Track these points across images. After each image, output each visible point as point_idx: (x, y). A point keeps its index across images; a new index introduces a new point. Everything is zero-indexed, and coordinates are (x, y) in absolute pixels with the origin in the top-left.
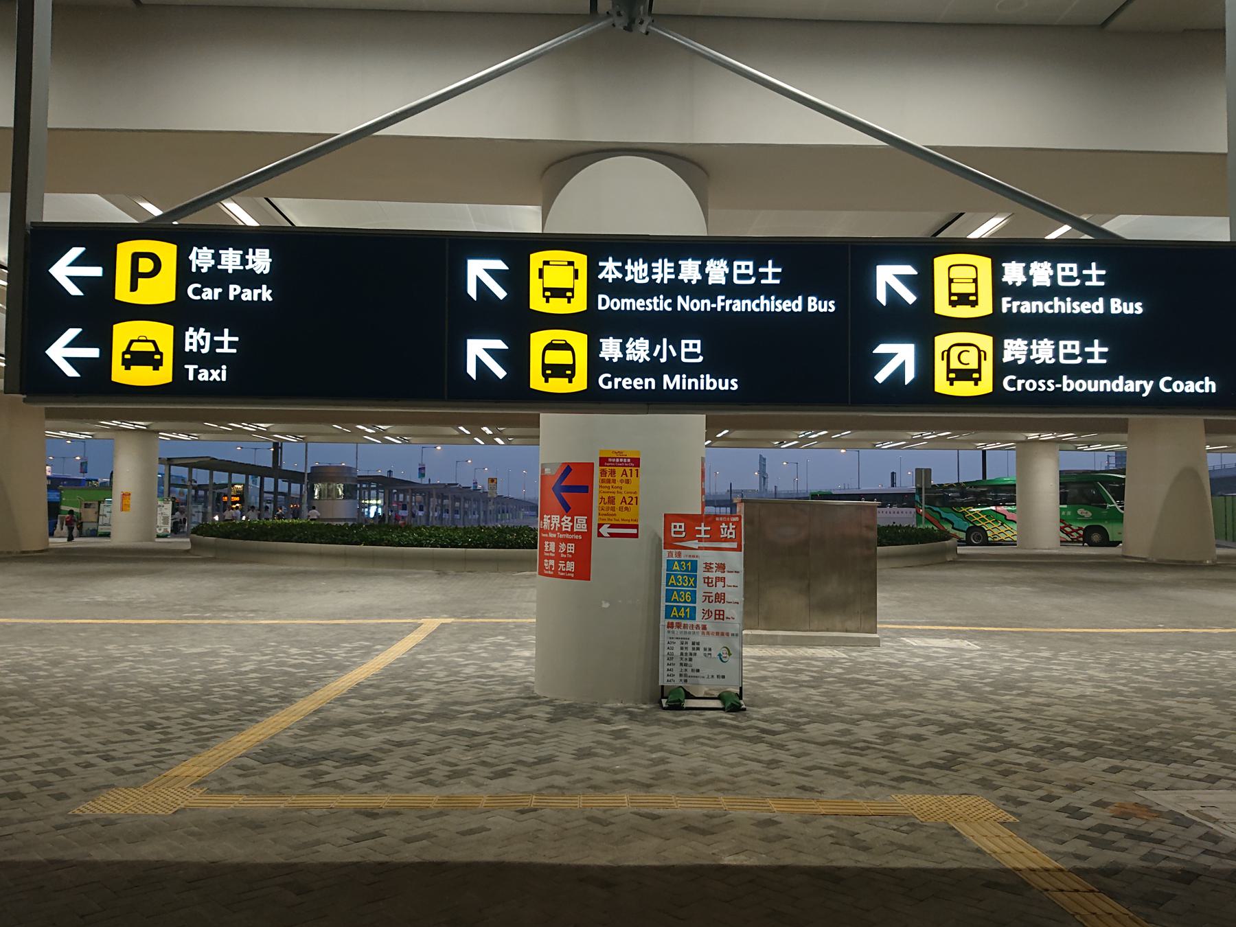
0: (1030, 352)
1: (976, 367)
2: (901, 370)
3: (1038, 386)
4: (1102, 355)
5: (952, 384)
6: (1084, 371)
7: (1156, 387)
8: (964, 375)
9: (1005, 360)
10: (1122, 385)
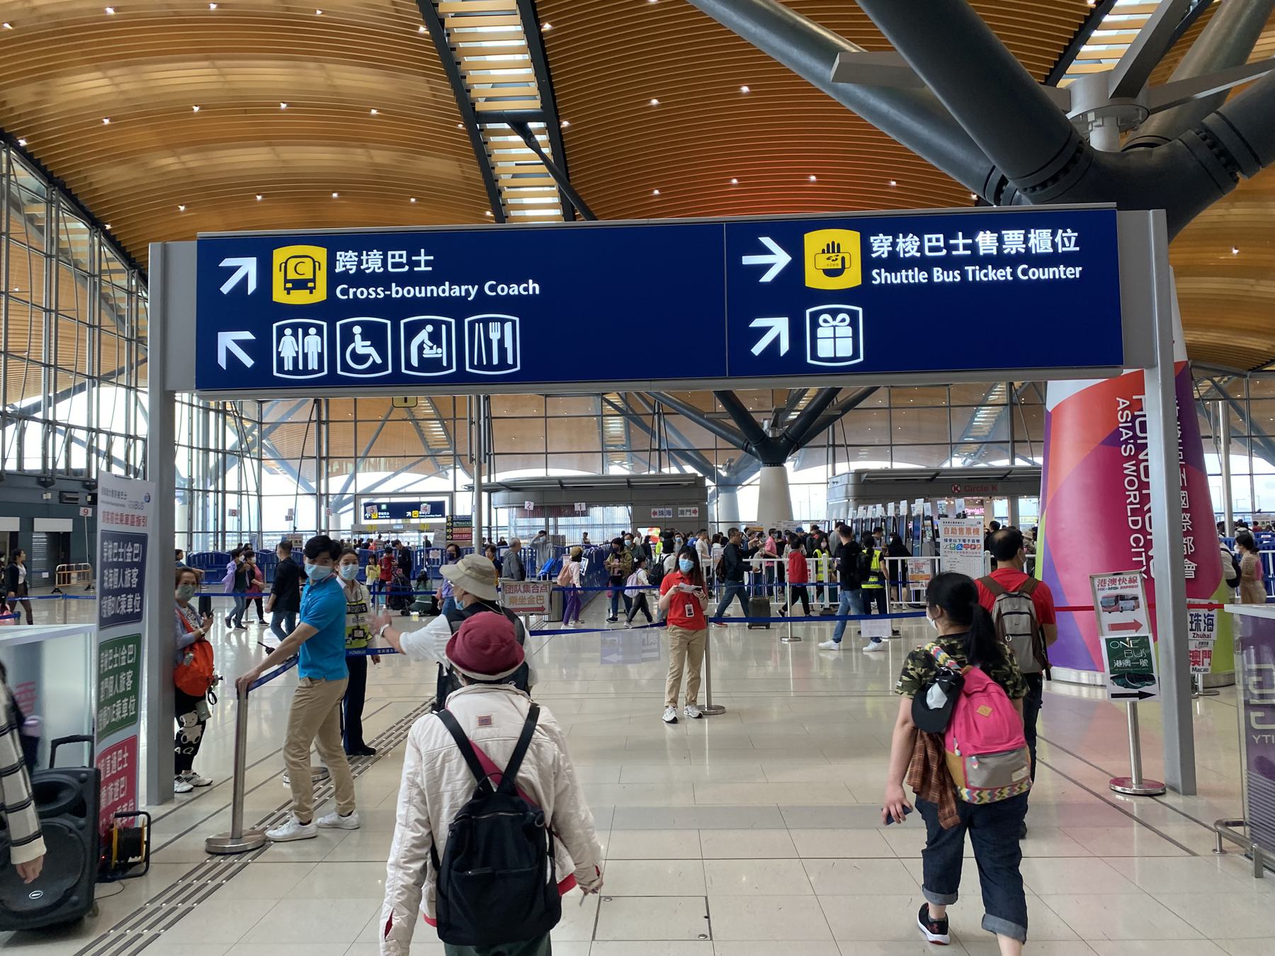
0: (360, 262)
3: (369, 294)
4: (427, 263)
5: (289, 293)
6: (411, 279)
7: (481, 292)
8: (300, 284)
9: (337, 271)
10: (447, 290)
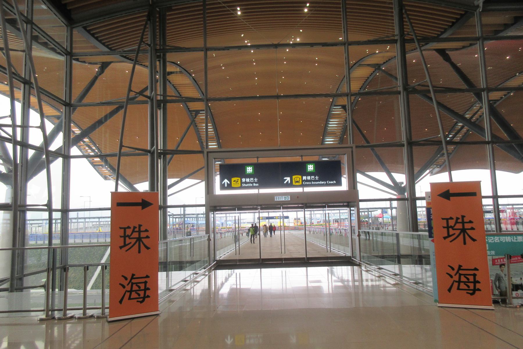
0: (307, 178)
1: (299, 180)
2: (288, 181)
4: (318, 178)
7: (326, 182)
8: (297, 182)
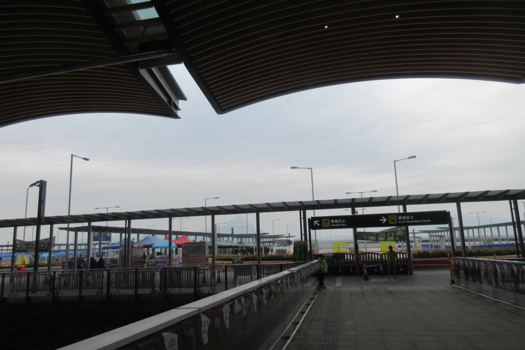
0: (402, 218)
6: (411, 220)
7: (421, 221)
